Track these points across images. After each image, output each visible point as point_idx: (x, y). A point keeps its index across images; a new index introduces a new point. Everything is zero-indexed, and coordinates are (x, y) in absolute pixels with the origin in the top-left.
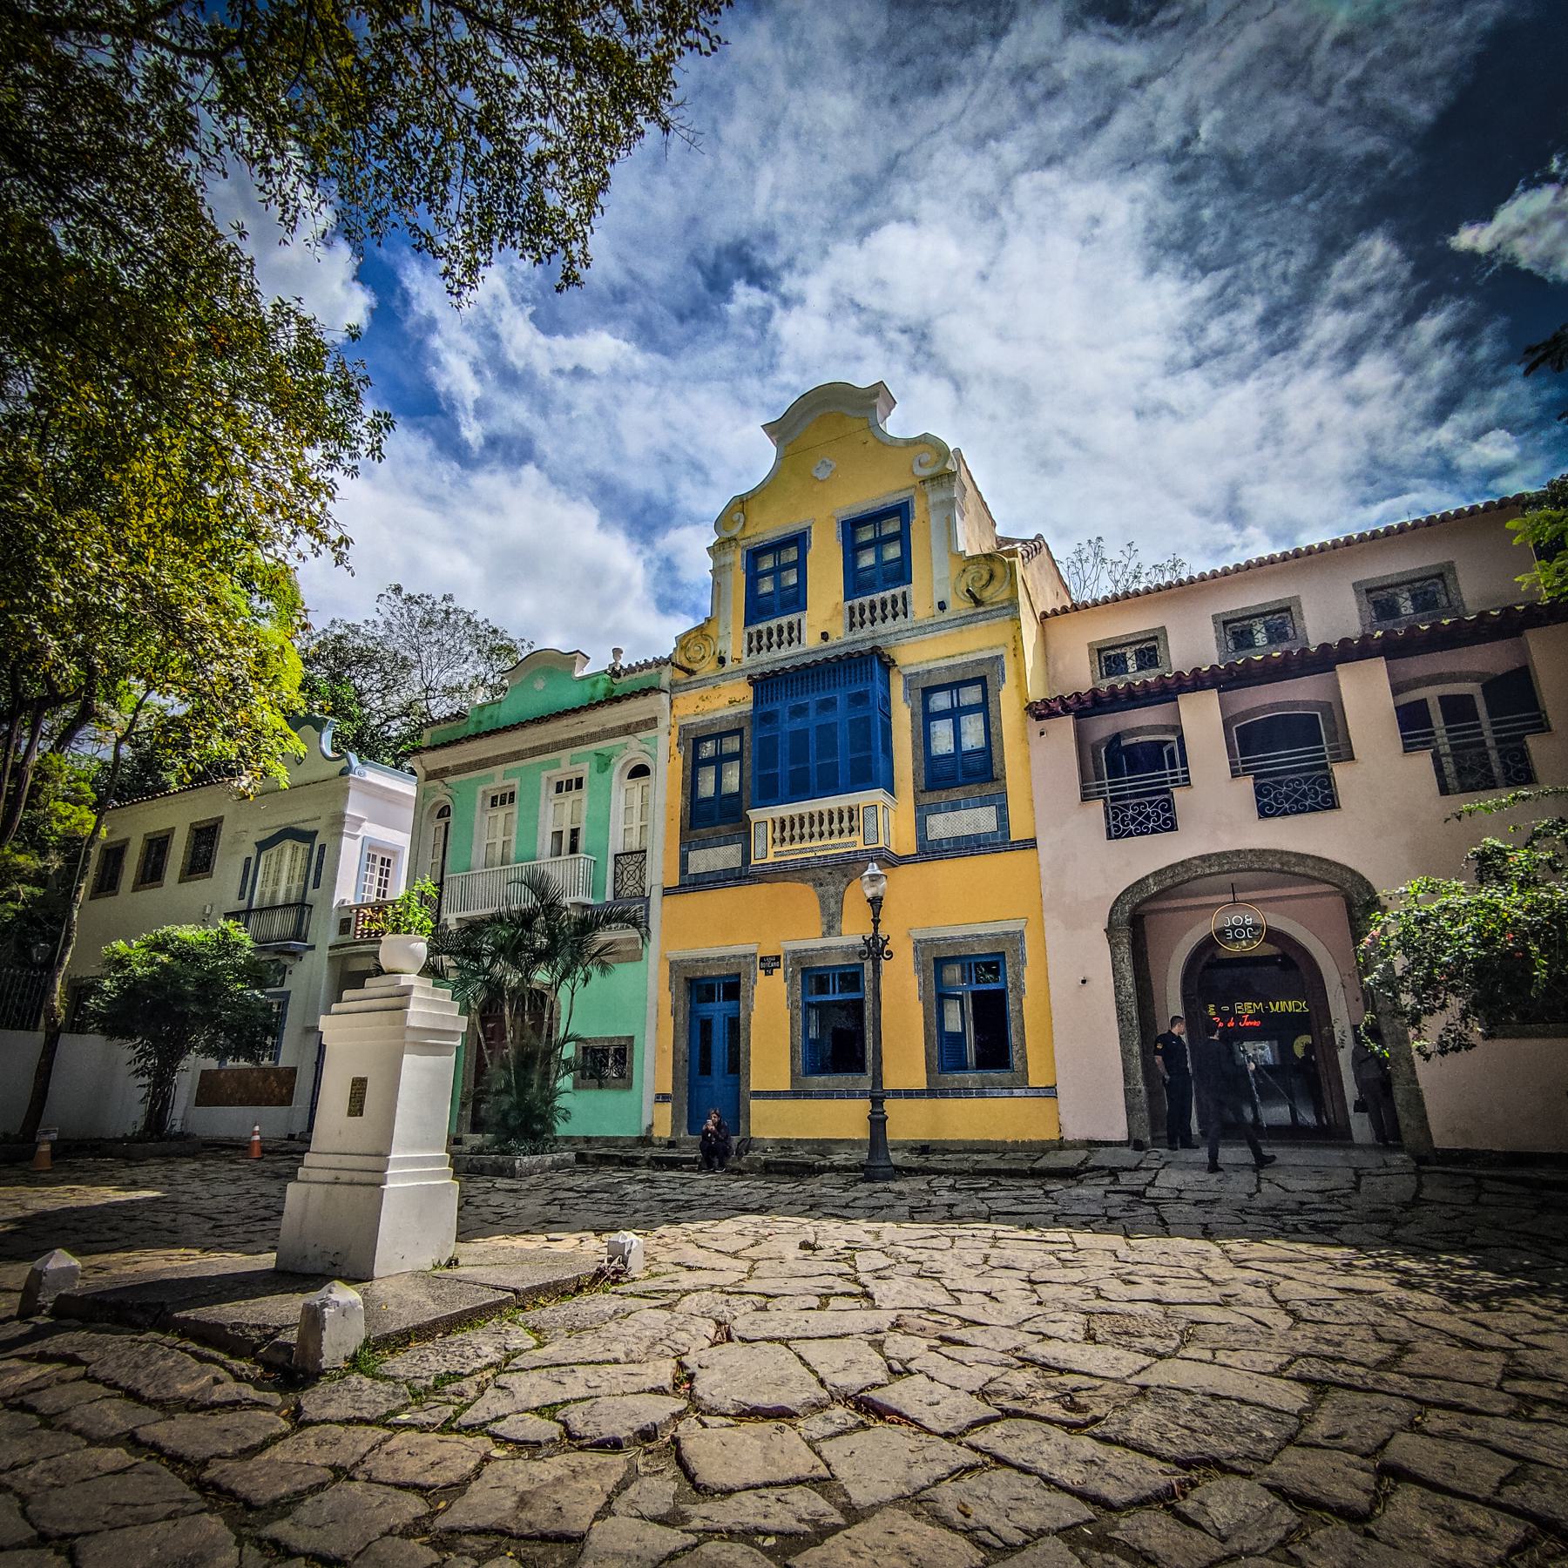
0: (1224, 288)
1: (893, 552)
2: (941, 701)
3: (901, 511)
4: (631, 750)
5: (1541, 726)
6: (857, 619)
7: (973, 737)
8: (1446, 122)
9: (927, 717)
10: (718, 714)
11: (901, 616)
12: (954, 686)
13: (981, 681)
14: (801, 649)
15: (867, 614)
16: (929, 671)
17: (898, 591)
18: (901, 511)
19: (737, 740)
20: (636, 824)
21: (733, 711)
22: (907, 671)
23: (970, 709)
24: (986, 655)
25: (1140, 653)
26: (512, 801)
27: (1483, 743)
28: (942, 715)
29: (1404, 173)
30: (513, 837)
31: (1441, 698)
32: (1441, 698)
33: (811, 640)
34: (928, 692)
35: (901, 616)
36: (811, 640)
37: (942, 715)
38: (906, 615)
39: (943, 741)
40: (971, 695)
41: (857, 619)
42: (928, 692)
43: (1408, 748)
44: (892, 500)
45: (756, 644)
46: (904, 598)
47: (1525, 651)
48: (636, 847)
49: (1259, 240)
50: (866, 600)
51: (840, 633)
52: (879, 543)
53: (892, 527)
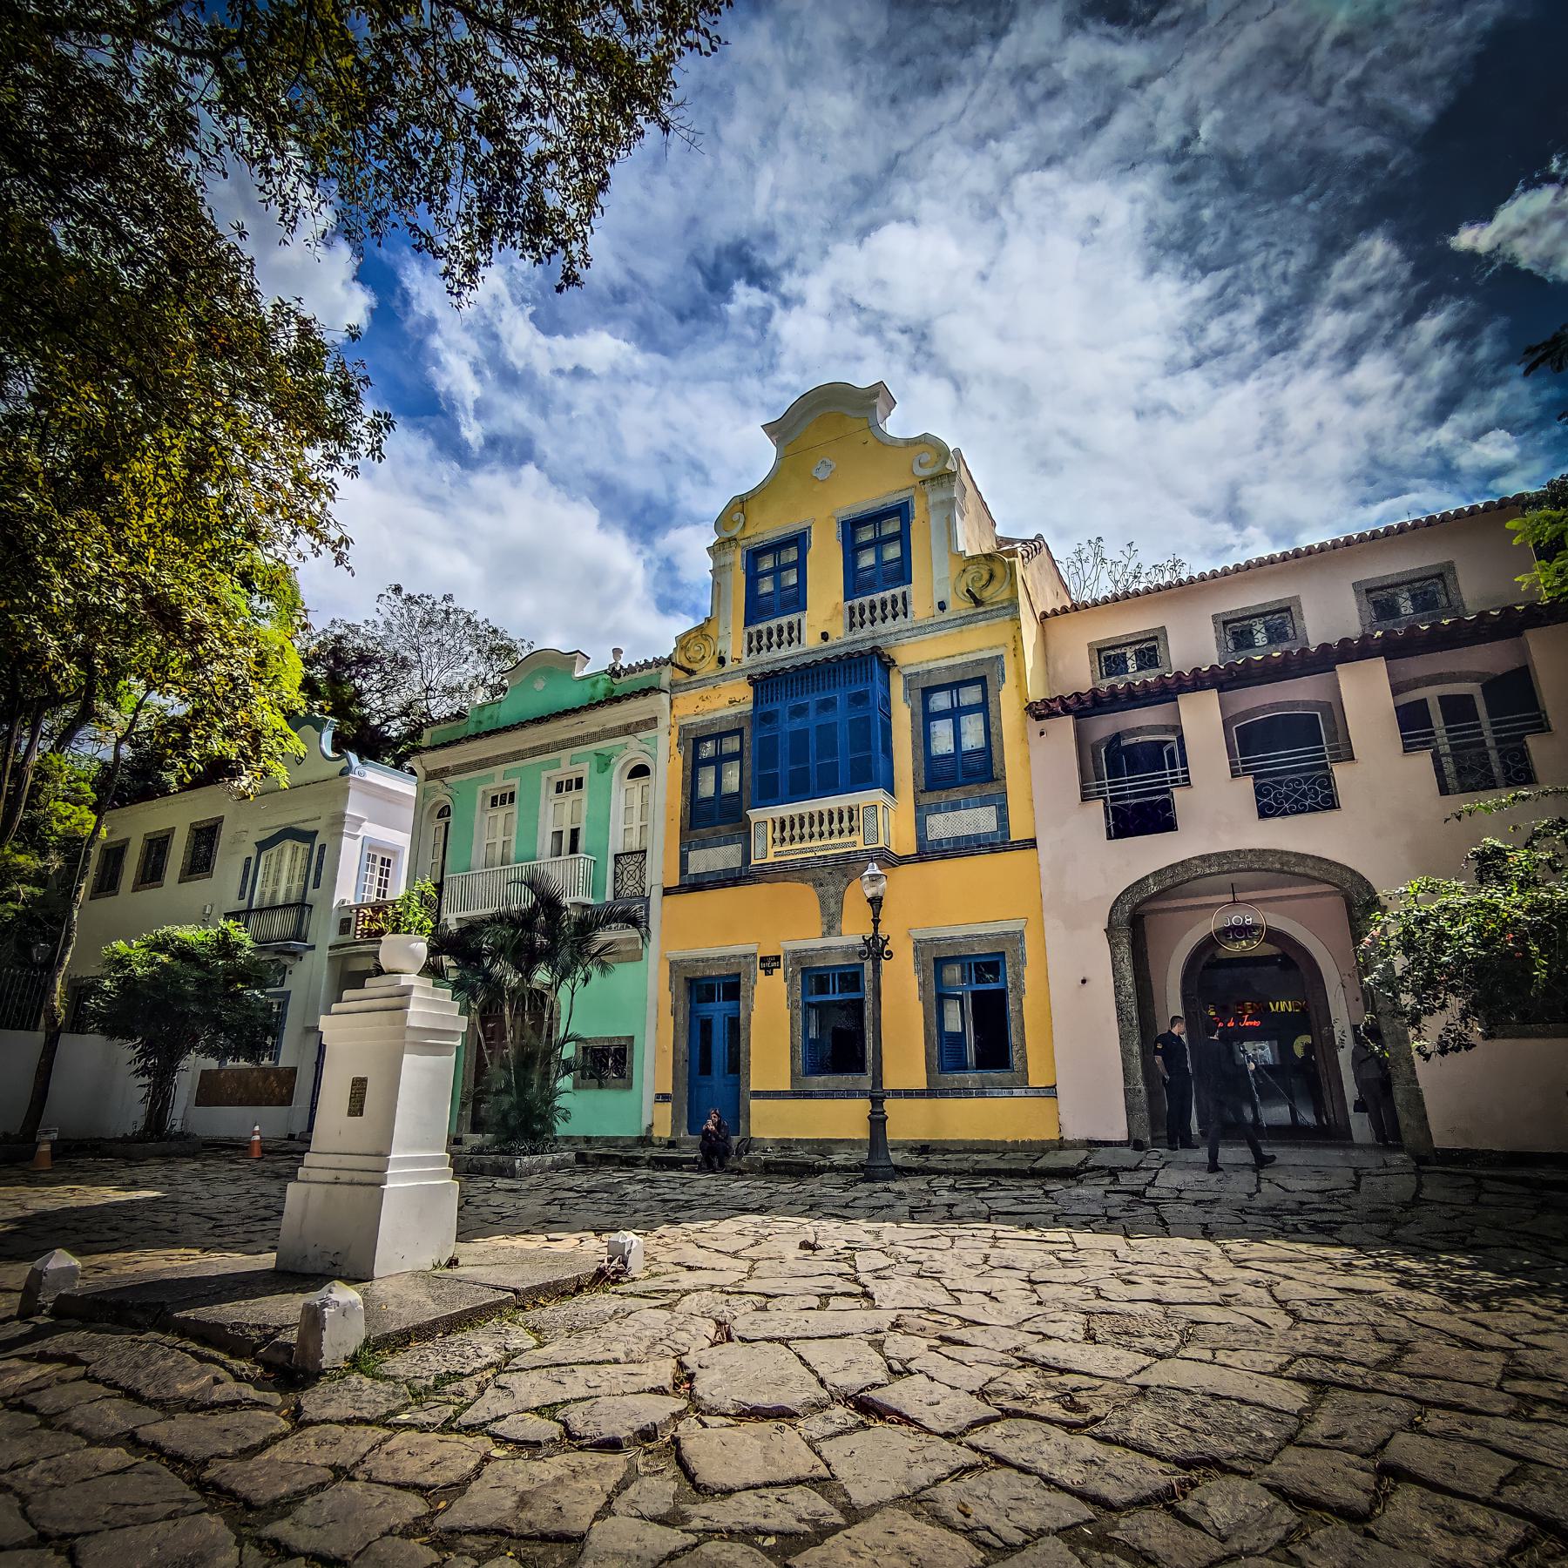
0: (1224, 288)
1: (893, 552)
2: (941, 701)
3: (901, 511)
4: (631, 750)
5: (1541, 726)
6: (857, 619)
7: (973, 737)
8: (1447, 120)
9: (927, 717)
10: (718, 714)
11: (901, 617)
12: (954, 686)
13: (981, 681)
14: (801, 650)
15: (867, 615)
16: (929, 671)
17: (898, 591)
18: (901, 511)
19: (737, 739)
20: (636, 824)
21: (734, 710)
22: (907, 671)
23: (970, 709)
24: (986, 655)
25: (1138, 653)
26: (512, 800)
27: (1483, 743)
28: (942, 715)
29: (1404, 173)
30: (514, 837)
31: (1441, 699)
32: (1441, 699)
33: (811, 640)
34: (927, 692)
35: (901, 617)
36: (811, 640)
37: (942, 715)
38: (905, 615)
39: (943, 741)
40: (971, 696)
41: (857, 619)
42: (927, 692)
43: (1408, 748)
44: (894, 499)
45: (755, 644)
46: (904, 598)
47: (1525, 651)
48: (636, 847)
49: (1260, 240)
50: (866, 600)
51: (839, 633)
52: (878, 543)
53: (891, 527)
